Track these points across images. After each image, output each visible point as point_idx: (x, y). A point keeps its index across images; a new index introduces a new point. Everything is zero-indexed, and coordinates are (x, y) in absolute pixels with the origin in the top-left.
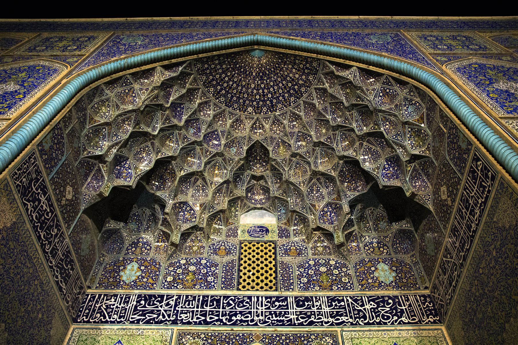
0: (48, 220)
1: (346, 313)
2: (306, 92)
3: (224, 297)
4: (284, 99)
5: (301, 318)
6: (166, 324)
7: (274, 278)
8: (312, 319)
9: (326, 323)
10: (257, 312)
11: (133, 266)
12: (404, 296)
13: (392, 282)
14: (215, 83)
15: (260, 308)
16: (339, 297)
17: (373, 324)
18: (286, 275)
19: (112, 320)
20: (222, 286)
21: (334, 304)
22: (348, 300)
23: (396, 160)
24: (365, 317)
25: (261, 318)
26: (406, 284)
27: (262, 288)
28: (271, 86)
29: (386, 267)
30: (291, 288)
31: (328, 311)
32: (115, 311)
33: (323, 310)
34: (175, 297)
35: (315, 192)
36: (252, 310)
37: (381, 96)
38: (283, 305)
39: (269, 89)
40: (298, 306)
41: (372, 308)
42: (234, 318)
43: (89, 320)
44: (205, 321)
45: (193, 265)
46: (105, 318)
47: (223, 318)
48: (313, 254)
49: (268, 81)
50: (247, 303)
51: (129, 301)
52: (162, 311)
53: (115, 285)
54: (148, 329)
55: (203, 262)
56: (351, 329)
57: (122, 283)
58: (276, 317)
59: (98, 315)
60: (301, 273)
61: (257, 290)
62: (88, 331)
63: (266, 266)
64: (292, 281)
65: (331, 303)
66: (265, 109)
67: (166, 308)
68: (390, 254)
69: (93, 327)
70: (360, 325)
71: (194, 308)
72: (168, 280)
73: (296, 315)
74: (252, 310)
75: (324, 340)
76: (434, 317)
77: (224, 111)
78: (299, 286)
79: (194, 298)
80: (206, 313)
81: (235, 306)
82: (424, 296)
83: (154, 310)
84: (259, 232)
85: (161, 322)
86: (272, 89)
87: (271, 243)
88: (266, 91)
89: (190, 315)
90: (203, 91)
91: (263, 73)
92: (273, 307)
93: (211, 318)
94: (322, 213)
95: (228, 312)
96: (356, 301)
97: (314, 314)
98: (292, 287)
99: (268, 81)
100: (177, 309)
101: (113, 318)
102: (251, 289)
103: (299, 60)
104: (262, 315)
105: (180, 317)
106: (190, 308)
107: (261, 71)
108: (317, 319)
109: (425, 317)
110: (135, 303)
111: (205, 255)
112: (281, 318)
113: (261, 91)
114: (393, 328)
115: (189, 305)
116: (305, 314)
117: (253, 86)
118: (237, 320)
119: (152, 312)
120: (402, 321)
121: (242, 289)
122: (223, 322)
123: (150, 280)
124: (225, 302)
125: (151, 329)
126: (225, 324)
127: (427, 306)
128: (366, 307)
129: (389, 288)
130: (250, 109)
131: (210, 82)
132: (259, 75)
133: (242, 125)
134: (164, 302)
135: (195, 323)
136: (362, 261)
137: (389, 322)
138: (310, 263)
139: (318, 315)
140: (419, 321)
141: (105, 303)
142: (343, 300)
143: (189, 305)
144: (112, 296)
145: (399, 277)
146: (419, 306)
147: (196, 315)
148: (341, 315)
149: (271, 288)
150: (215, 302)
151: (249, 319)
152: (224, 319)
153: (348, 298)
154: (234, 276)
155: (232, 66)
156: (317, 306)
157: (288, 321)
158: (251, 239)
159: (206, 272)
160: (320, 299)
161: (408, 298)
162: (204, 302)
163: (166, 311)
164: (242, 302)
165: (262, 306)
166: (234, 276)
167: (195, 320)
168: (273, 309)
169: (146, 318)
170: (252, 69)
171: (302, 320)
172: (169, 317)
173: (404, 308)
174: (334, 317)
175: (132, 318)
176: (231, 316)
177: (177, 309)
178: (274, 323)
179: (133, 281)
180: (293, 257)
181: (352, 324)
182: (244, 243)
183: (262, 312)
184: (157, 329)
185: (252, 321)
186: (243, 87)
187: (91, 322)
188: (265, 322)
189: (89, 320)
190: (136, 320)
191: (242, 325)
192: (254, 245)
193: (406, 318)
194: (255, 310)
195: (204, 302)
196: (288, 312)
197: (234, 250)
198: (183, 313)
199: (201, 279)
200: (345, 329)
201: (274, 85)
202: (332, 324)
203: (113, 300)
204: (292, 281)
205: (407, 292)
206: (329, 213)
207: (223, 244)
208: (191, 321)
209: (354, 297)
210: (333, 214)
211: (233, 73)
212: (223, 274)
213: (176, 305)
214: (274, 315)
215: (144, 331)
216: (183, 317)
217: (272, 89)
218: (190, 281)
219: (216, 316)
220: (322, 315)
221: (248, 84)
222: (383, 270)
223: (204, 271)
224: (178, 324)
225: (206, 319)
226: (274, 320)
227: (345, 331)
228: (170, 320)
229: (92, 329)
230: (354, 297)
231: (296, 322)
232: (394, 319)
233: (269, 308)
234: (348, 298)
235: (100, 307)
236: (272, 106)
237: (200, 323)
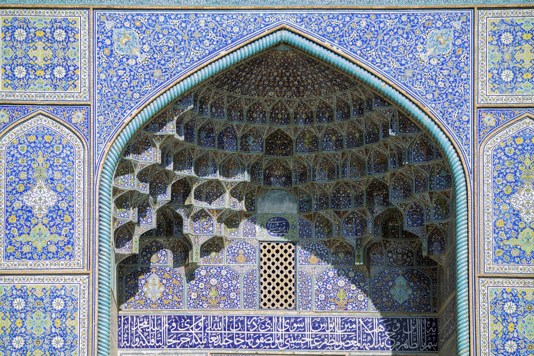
1: (356, 336)
3: (248, 318)
6: (199, 347)
8: (325, 343)
9: (337, 347)
10: (277, 334)
11: (154, 279)
13: (406, 301)
16: (352, 318)
17: (377, 349)
18: (305, 290)
19: (151, 344)
20: (245, 304)
21: (346, 326)
22: (359, 322)
25: (281, 341)
30: (309, 307)
31: (340, 334)
33: (336, 333)
34: (203, 319)
38: (301, 327)
40: (313, 328)
41: (380, 332)
42: (257, 341)
44: (233, 344)
45: (214, 277)
46: (144, 342)
47: (248, 341)
50: (268, 324)
51: (161, 323)
52: (194, 334)
57: (149, 302)
59: (137, 340)
60: (319, 287)
64: (310, 298)
65: (344, 325)
67: (197, 330)
68: (412, 265)
69: (137, 352)
70: (366, 349)
71: (221, 330)
73: (312, 338)
74: (274, 333)
78: (316, 305)
79: (221, 318)
80: (233, 336)
83: (186, 333)
84: (278, 226)
85: (195, 346)
92: (291, 329)
93: (238, 341)
94: (346, 220)
98: (310, 306)
100: (207, 331)
104: (282, 338)
105: (211, 340)
106: (218, 330)
108: (330, 343)
110: (167, 325)
112: (299, 342)
115: (216, 327)
116: (320, 337)
118: (260, 343)
119: (185, 335)
124: (249, 323)
126: (250, 347)
133: (260, 107)
134: (194, 324)
138: (329, 274)
140: (419, 348)
141: (140, 327)
144: (143, 317)
145: (414, 295)
147: (225, 338)
150: (240, 324)
152: (249, 341)
153: (360, 320)
154: (255, 292)
156: (331, 328)
157: (304, 344)
159: (227, 286)
160: (334, 321)
161: (415, 321)
162: (230, 325)
163: (197, 334)
165: (282, 328)
166: (255, 292)
167: (224, 343)
169: (181, 342)
171: (316, 344)
172: (201, 341)
173: (408, 333)
174: (345, 341)
175: (168, 342)
176: (255, 339)
177: (207, 331)
178: (293, 346)
179: (159, 299)
180: (313, 266)
181: (359, 349)
183: (282, 334)
185: (274, 344)
187: (133, 347)
188: (285, 345)
190: (173, 344)
191: (265, 348)
193: (408, 344)
195: (230, 325)
196: (305, 334)
198: (212, 336)
202: (341, 349)
203: (146, 322)
204: (310, 298)
207: (241, 247)
208: (221, 344)
209: (366, 319)
212: (245, 289)
213: (205, 328)
214: (292, 338)
216: (213, 341)
218: (214, 299)
219: (242, 338)
220: (334, 339)
221: (270, 73)
223: (225, 285)
224: (209, 347)
225: (233, 342)
226: (292, 343)
228: (202, 344)
230: (366, 319)
231: (311, 346)
232: (397, 344)
233: (288, 330)
235: (136, 330)
237: (229, 347)
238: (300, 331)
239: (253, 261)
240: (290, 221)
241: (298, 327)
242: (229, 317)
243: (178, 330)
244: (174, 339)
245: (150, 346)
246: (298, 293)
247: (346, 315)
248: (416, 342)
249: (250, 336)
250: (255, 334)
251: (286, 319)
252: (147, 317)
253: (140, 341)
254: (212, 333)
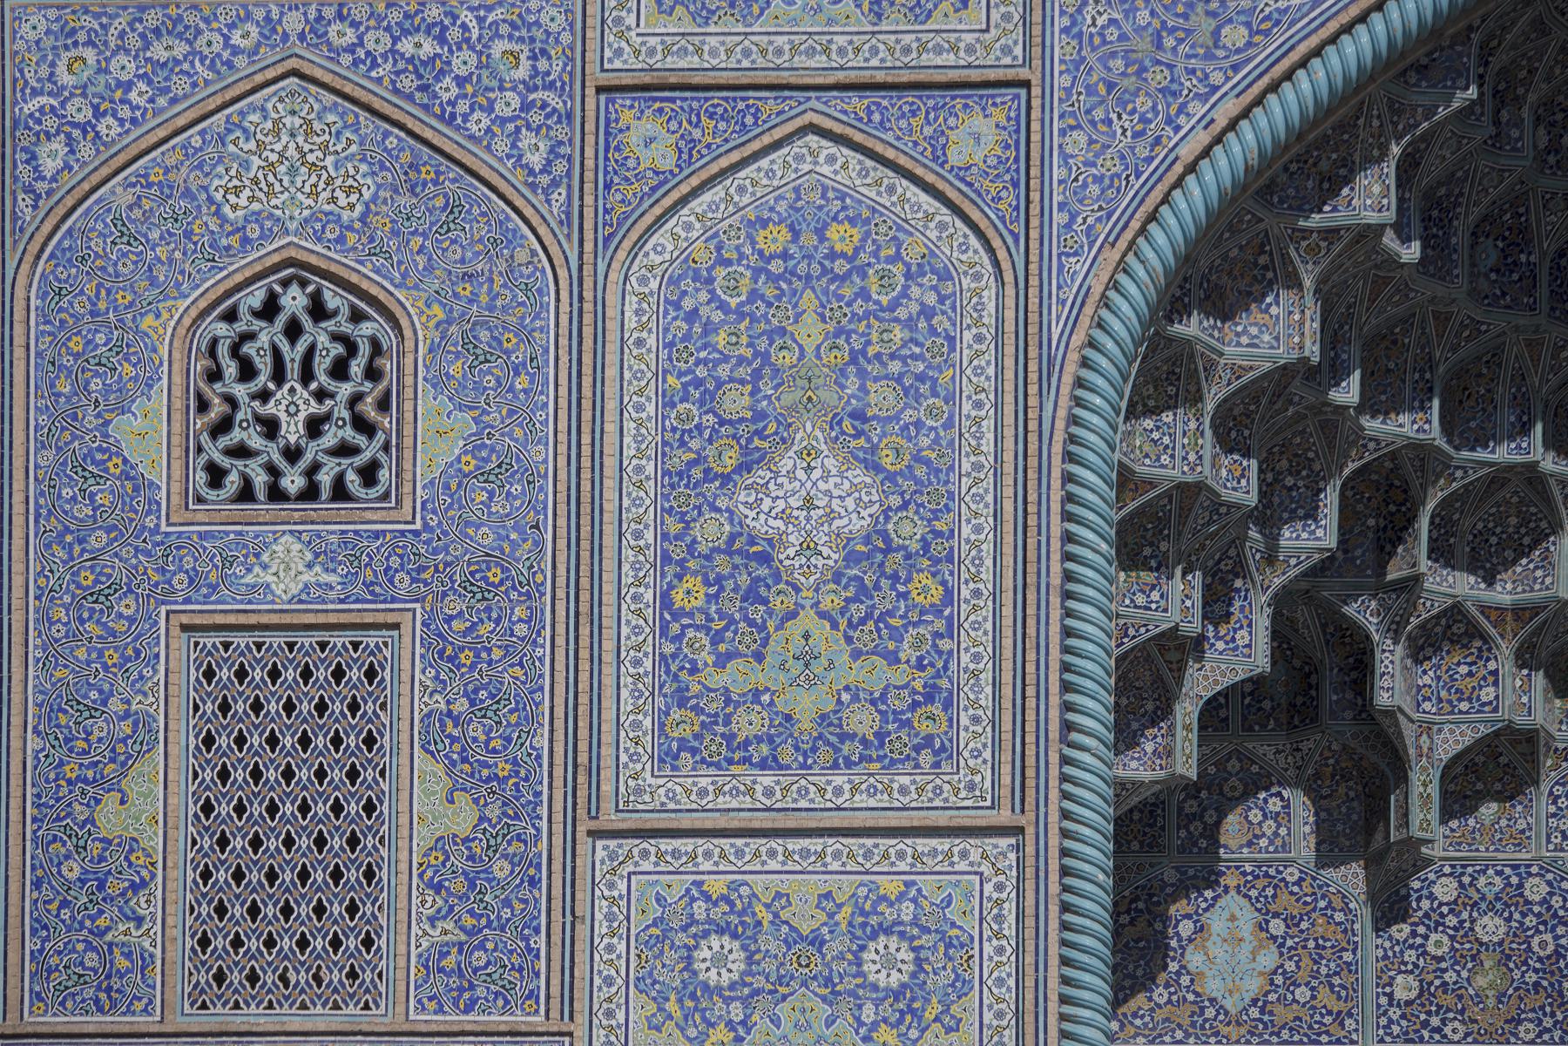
53: (1186, 1022)
55: (1535, 889)
57: (1210, 1013)
72: (1401, 994)
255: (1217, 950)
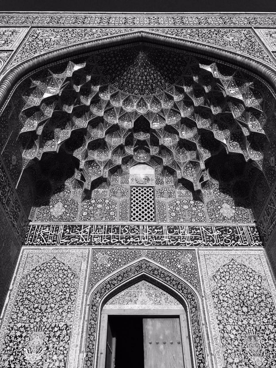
0: (3, 182)
1: (201, 238)
2: (178, 79)
3: (122, 226)
4: (161, 84)
5: (172, 240)
6: (84, 245)
7: (154, 213)
8: (179, 241)
9: (188, 244)
12: (240, 227)
13: (232, 217)
14: (111, 71)
15: (145, 233)
17: (219, 245)
19: (48, 243)
20: (120, 218)
21: (193, 231)
22: (202, 229)
23: (240, 134)
24: (213, 241)
25: (146, 240)
26: (241, 218)
27: (146, 219)
28: (152, 74)
29: (229, 206)
31: (189, 236)
32: (50, 237)
33: (186, 235)
34: (89, 227)
35: (181, 153)
36: (140, 235)
37: (233, 86)
38: (160, 232)
39: (150, 76)
40: (169, 232)
42: (128, 240)
43: (33, 243)
44: (110, 242)
45: (100, 204)
46: (43, 241)
48: (180, 196)
49: (150, 69)
50: (136, 230)
51: (58, 230)
52: (82, 236)
53: (48, 219)
54: (73, 249)
56: (204, 248)
57: (52, 217)
58: (156, 239)
59: (39, 240)
61: (143, 221)
62: (33, 250)
63: (148, 204)
64: (165, 215)
65: (191, 230)
66: (147, 91)
67: (84, 234)
69: (36, 248)
70: (210, 246)
71: (102, 234)
72: (84, 214)
73: (169, 238)
74: (140, 235)
75: (187, 255)
76: (259, 242)
77: (118, 92)
79: (102, 226)
80: (110, 237)
81: (129, 232)
82: (253, 227)
86: (152, 76)
87: (151, 188)
88: (148, 77)
89: (99, 238)
90: (102, 78)
91: (146, 64)
92: (153, 233)
93: (114, 241)
94: (185, 168)
95: (124, 236)
96: (207, 229)
97: (180, 238)
98: (165, 219)
99: (150, 69)
100: (91, 234)
101: (49, 242)
102: (139, 220)
103: (173, 55)
104: (146, 239)
105: (94, 240)
106: (100, 234)
107: (144, 62)
109: (253, 242)
110: (63, 231)
111: (108, 196)
112: (159, 241)
113: (144, 78)
114: (231, 249)
115: (99, 232)
117: (138, 73)
118: (130, 242)
119: (75, 237)
120: (237, 244)
121: (133, 220)
122: (121, 243)
123: (72, 215)
124: (122, 229)
125: (75, 249)
126: (123, 245)
127: (255, 234)
128: (214, 234)
129: (230, 221)
130: (136, 91)
131: (107, 71)
132: (143, 65)
134: (82, 230)
135: (104, 244)
136: (212, 202)
137: (229, 245)
139: (183, 239)
140: (249, 244)
141: (42, 232)
142: (199, 229)
143: (99, 232)
144: (46, 226)
146: (250, 234)
147: (104, 238)
148: (198, 239)
149: (152, 219)
150: (116, 230)
151: (138, 241)
152: (122, 241)
153: (203, 228)
155: (123, 58)
156: (182, 232)
157: (163, 243)
158: (138, 185)
160: (184, 228)
161: (242, 228)
163: (84, 236)
164: (133, 229)
165: (146, 232)
167: (103, 242)
168: (153, 234)
170: (138, 60)
171: (172, 242)
172: (86, 241)
173: (239, 235)
174: (193, 240)
175: (61, 242)
176: (126, 239)
177: (91, 234)
181: (205, 245)
182: (133, 188)
183: (146, 236)
184: (79, 249)
185: (140, 242)
186: (131, 74)
187: (34, 245)
188: (149, 243)
189: (33, 243)
190: (65, 243)
191: (134, 245)
192: (140, 190)
194: (142, 235)
195: (109, 230)
197: (126, 193)
198: (95, 237)
199: (106, 213)
200: (200, 248)
201: (154, 73)
202: (192, 245)
203: (47, 229)
204: (165, 215)
205: (242, 224)
206: (190, 168)
207: (119, 189)
209: (206, 227)
210: (193, 169)
211: (124, 63)
213: (90, 232)
215: (71, 250)
216: (96, 240)
217: (152, 76)
219: (116, 239)
220: (185, 239)
221: (135, 72)
222: (226, 208)
223: (107, 208)
225: (110, 241)
226: (154, 242)
227: (200, 250)
228: (87, 242)
229: (36, 249)
231: (168, 243)
232: (233, 243)
233: (151, 234)
234: (203, 228)
235: (39, 234)
236: (153, 89)
237: (107, 244)
238: (159, 234)
239: (127, 196)
240: (150, 178)
241: (158, 231)
242: (108, 226)
243: (70, 234)
244: (66, 240)
245: (47, 244)
246: (157, 212)
247: (191, 224)
248: (246, 240)
249: (123, 237)
250: (126, 236)
251: (149, 227)
252: (49, 226)
253: (40, 241)
254: (95, 236)
255: (55, 209)
